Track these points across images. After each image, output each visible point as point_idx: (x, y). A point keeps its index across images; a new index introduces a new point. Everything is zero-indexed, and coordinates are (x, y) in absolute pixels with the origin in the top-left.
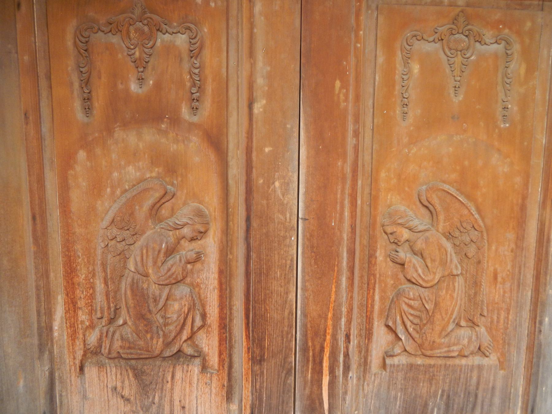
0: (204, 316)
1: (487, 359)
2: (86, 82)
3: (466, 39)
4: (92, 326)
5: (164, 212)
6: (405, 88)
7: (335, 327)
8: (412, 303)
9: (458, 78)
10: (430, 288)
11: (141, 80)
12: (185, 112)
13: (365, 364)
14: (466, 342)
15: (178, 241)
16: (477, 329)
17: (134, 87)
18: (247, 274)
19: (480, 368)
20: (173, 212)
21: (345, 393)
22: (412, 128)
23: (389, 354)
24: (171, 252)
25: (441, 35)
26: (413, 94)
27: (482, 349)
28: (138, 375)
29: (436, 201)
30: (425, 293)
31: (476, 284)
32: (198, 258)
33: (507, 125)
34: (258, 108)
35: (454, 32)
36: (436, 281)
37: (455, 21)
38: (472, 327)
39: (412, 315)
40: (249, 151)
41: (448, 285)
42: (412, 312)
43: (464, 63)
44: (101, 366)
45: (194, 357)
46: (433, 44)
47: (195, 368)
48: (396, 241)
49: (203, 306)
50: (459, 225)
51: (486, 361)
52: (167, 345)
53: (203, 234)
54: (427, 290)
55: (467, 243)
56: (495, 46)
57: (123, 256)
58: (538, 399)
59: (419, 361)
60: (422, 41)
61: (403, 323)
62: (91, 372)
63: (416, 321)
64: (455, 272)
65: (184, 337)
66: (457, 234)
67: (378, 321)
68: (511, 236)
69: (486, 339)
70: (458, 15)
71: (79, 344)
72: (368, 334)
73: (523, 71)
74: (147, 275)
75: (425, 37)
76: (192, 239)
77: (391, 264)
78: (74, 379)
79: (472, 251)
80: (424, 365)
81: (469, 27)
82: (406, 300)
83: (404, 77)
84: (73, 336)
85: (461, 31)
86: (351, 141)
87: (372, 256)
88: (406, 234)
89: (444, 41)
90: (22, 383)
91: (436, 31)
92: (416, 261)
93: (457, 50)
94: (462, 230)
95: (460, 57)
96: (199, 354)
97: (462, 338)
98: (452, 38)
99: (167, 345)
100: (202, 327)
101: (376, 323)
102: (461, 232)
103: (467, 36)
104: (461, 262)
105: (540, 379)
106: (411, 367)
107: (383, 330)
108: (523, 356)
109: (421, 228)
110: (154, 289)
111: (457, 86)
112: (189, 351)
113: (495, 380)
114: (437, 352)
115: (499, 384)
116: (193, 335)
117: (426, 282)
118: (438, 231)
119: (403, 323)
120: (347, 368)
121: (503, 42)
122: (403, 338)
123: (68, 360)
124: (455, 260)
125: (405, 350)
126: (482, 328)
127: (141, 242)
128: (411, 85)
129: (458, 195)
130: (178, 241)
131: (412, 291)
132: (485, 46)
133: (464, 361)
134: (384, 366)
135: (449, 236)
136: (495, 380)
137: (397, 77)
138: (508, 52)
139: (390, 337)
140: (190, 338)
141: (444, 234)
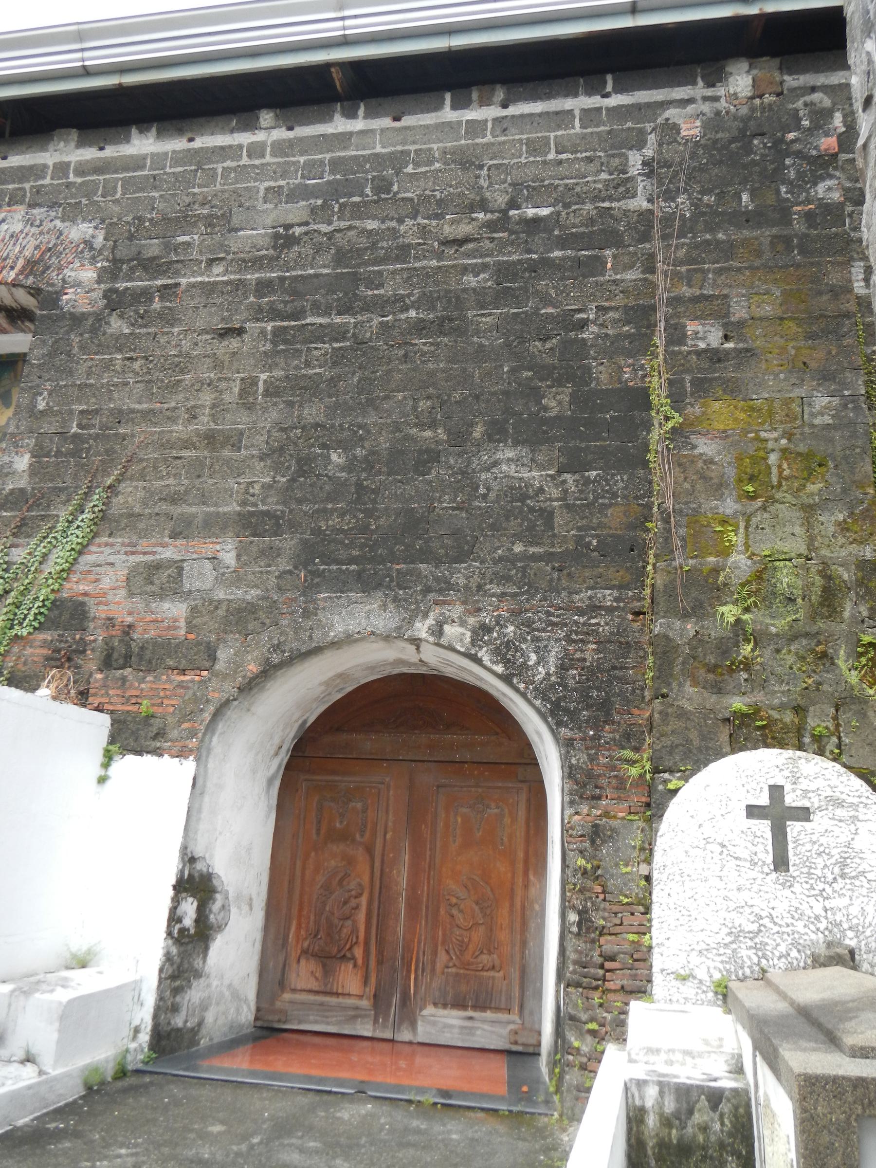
0: (357, 937)
2: (319, 822)
4: (306, 939)
5: (345, 883)
7: (418, 947)
11: (341, 822)
12: (358, 836)
13: (433, 970)
15: (350, 897)
17: (338, 825)
18: (378, 915)
19: (493, 978)
20: (348, 883)
24: (345, 903)
26: (458, 831)
28: (324, 966)
30: (465, 933)
31: (491, 930)
32: (357, 907)
34: (388, 836)
40: (383, 855)
44: (307, 959)
45: (350, 959)
47: (351, 966)
49: (358, 931)
51: (497, 975)
52: (339, 951)
53: (359, 896)
56: (496, 811)
57: (324, 904)
59: (462, 971)
62: (303, 962)
65: (348, 947)
68: (507, 904)
69: (497, 963)
71: (299, 946)
72: (435, 953)
74: (333, 914)
76: (356, 897)
78: (294, 965)
79: (488, 912)
84: (297, 942)
86: (428, 853)
87: (438, 911)
88: (454, 900)
90: (271, 964)
92: (460, 916)
96: (353, 958)
99: (339, 951)
100: (356, 943)
106: (457, 974)
107: (444, 952)
108: (517, 973)
110: (336, 921)
112: (349, 955)
114: (471, 967)
115: (504, 988)
116: (350, 949)
123: (293, 954)
124: (480, 915)
127: (333, 897)
130: (350, 897)
131: (458, 932)
133: (485, 973)
134: (443, 973)
135: (477, 903)
139: (447, 957)
140: (350, 949)
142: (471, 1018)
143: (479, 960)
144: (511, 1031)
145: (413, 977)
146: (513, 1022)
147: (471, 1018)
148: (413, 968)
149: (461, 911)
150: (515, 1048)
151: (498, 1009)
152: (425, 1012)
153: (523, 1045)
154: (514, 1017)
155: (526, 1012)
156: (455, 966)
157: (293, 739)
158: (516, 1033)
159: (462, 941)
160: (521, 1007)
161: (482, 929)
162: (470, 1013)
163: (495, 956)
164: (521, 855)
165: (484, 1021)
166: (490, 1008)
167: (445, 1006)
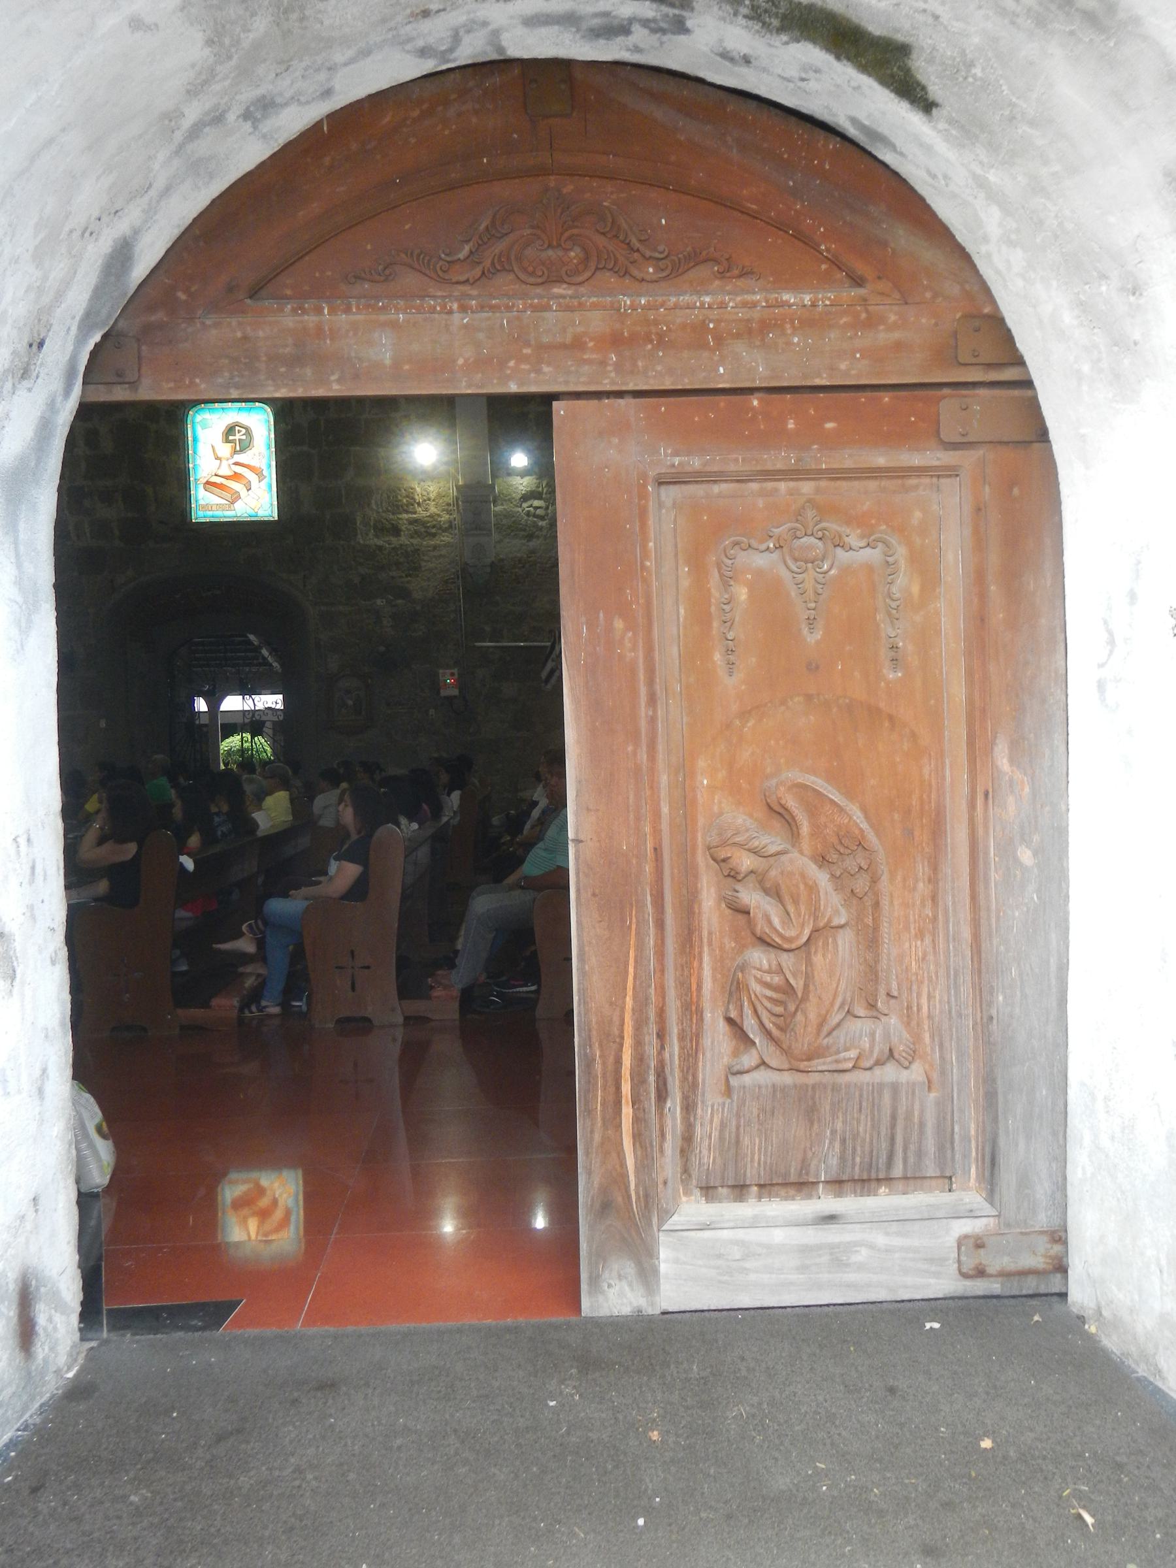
1: (905, 1073)
3: (820, 544)
6: (728, 624)
8: (767, 978)
9: (813, 605)
10: (796, 952)
14: (866, 1043)
16: (883, 1019)
19: (895, 1088)
21: (663, 1135)
22: (743, 687)
23: (735, 1069)
25: (779, 540)
27: (896, 1055)
29: (791, 803)
30: (787, 960)
33: (900, 675)
35: (798, 533)
36: (805, 939)
37: (799, 518)
38: (876, 1018)
39: (770, 999)
41: (826, 944)
42: (769, 993)
43: (819, 580)
46: (766, 554)
48: (732, 874)
50: (836, 842)
51: (904, 1076)
54: (791, 954)
55: (852, 872)
56: (868, 550)
58: (1002, 1142)
60: (750, 551)
61: (755, 1011)
63: (779, 1010)
64: (836, 922)
66: (834, 857)
67: (712, 1012)
70: (803, 508)
73: (915, 589)
75: (754, 543)
77: (728, 911)
80: (795, 1086)
81: (824, 525)
82: (759, 974)
83: (725, 607)
85: (809, 532)
88: (746, 862)
89: (784, 549)
91: (771, 534)
93: (806, 562)
94: (842, 851)
95: (811, 571)
97: (857, 1034)
98: (797, 543)
101: (708, 1015)
102: (841, 854)
103: (820, 539)
104: (847, 904)
105: (1000, 1105)
107: (722, 1025)
109: (773, 849)
111: (812, 617)
113: (922, 1112)
117: (789, 940)
118: (801, 852)
119: (755, 1011)
120: (662, 1095)
121: (880, 544)
122: (757, 1041)
125: (763, 1063)
126: (891, 1018)
128: (737, 619)
129: (829, 792)
132: (851, 552)
134: (728, 1091)
135: (822, 860)
136: (922, 1112)
137: (713, 609)
138: (889, 559)
141: (813, 858)
142: (831, 1218)
143: (841, 1036)
144: (961, 1242)
145: (627, 1111)
146: (971, 1214)
147: (831, 1218)
148: (626, 1088)
149: (774, 892)
150: (979, 1287)
151: (913, 1179)
152: (676, 1221)
153: (1005, 1275)
154: (973, 1197)
155: (1008, 1178)
156: (763, 1063)
157: (87, 322)
158: (979, 1244)
159: (788, 989)
160: (991, 1164)
161: (845, 942)
162: (827, 1203)
163: (893, 1021)
164: (957, 691)
165: (877, 1221)
166: (888, 1180)
167: (740, 1190)
